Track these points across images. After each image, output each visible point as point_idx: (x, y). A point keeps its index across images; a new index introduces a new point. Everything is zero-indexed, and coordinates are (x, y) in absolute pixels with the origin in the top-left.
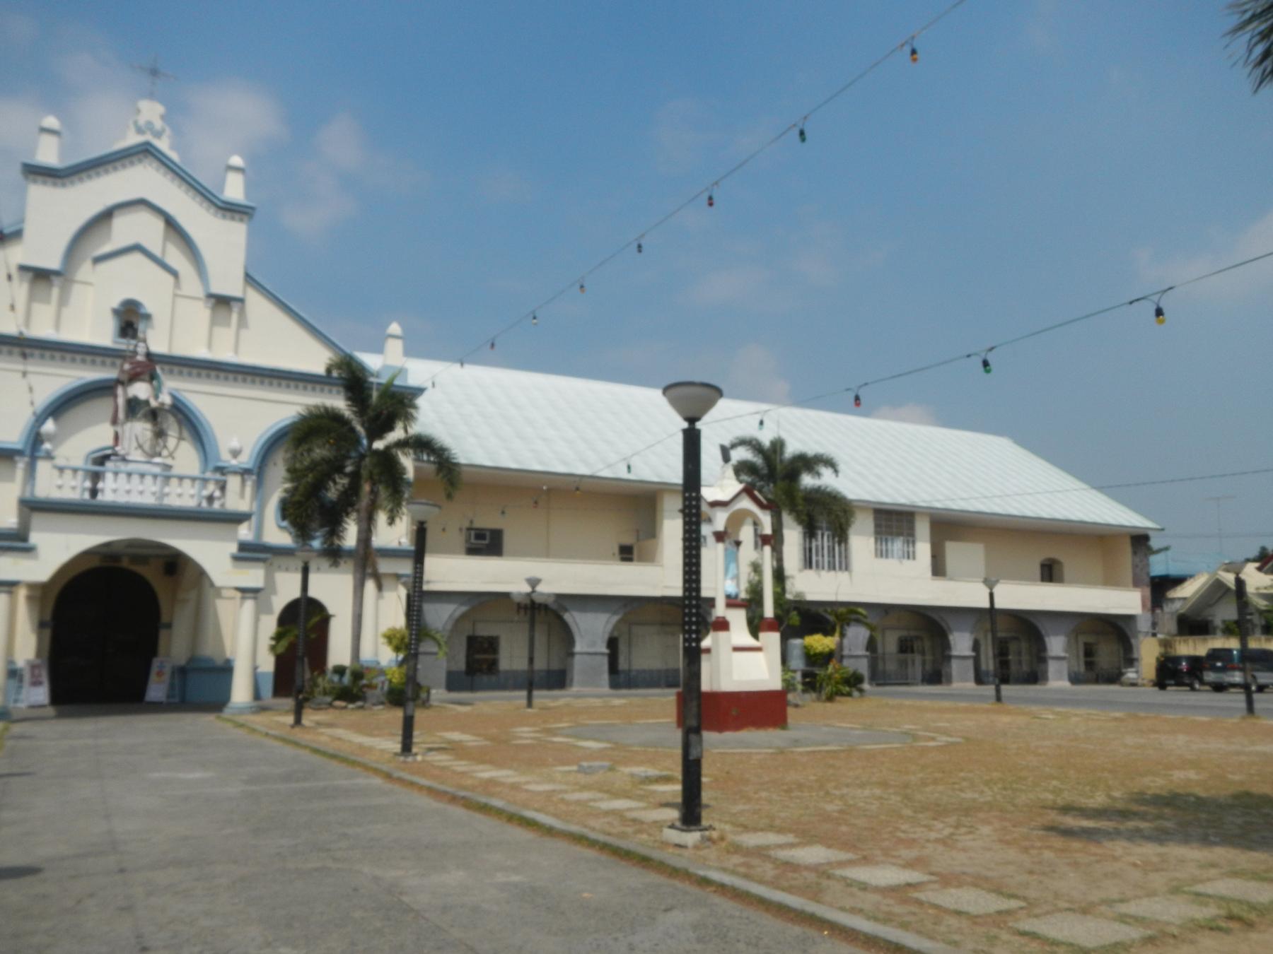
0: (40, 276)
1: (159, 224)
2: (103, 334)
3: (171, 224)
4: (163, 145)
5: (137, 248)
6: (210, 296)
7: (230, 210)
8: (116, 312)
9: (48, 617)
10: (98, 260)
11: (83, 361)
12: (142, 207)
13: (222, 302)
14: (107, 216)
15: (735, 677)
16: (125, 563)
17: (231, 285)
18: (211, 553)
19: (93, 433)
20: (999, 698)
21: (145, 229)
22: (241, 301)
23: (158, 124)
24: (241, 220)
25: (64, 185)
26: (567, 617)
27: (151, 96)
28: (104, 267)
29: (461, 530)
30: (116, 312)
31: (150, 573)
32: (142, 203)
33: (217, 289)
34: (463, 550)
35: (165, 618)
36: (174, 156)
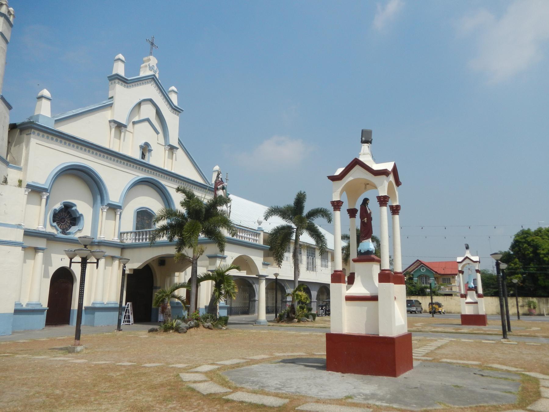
0: (120, 126)
1: (154, 111)
3: (159, 113)
4: (157, 76)
5: (148, 120)
6: (170, 145)
7: (176, 110)
8: (141, 147)
10: (134, 123)
11: (136, 168)
12: (149, 102)
13: (172, 148)
14: (139, 104)
15: (365, 308)
17: (174, 142)
20: (433, 316)
22: (177, 148)
23: (155, 68)
24: (178, 115)
25: (128, 87)
26: (254, 286)
27: (151, 54)
28: (137, 126)
30: (141, 147)
32: (151, 101)
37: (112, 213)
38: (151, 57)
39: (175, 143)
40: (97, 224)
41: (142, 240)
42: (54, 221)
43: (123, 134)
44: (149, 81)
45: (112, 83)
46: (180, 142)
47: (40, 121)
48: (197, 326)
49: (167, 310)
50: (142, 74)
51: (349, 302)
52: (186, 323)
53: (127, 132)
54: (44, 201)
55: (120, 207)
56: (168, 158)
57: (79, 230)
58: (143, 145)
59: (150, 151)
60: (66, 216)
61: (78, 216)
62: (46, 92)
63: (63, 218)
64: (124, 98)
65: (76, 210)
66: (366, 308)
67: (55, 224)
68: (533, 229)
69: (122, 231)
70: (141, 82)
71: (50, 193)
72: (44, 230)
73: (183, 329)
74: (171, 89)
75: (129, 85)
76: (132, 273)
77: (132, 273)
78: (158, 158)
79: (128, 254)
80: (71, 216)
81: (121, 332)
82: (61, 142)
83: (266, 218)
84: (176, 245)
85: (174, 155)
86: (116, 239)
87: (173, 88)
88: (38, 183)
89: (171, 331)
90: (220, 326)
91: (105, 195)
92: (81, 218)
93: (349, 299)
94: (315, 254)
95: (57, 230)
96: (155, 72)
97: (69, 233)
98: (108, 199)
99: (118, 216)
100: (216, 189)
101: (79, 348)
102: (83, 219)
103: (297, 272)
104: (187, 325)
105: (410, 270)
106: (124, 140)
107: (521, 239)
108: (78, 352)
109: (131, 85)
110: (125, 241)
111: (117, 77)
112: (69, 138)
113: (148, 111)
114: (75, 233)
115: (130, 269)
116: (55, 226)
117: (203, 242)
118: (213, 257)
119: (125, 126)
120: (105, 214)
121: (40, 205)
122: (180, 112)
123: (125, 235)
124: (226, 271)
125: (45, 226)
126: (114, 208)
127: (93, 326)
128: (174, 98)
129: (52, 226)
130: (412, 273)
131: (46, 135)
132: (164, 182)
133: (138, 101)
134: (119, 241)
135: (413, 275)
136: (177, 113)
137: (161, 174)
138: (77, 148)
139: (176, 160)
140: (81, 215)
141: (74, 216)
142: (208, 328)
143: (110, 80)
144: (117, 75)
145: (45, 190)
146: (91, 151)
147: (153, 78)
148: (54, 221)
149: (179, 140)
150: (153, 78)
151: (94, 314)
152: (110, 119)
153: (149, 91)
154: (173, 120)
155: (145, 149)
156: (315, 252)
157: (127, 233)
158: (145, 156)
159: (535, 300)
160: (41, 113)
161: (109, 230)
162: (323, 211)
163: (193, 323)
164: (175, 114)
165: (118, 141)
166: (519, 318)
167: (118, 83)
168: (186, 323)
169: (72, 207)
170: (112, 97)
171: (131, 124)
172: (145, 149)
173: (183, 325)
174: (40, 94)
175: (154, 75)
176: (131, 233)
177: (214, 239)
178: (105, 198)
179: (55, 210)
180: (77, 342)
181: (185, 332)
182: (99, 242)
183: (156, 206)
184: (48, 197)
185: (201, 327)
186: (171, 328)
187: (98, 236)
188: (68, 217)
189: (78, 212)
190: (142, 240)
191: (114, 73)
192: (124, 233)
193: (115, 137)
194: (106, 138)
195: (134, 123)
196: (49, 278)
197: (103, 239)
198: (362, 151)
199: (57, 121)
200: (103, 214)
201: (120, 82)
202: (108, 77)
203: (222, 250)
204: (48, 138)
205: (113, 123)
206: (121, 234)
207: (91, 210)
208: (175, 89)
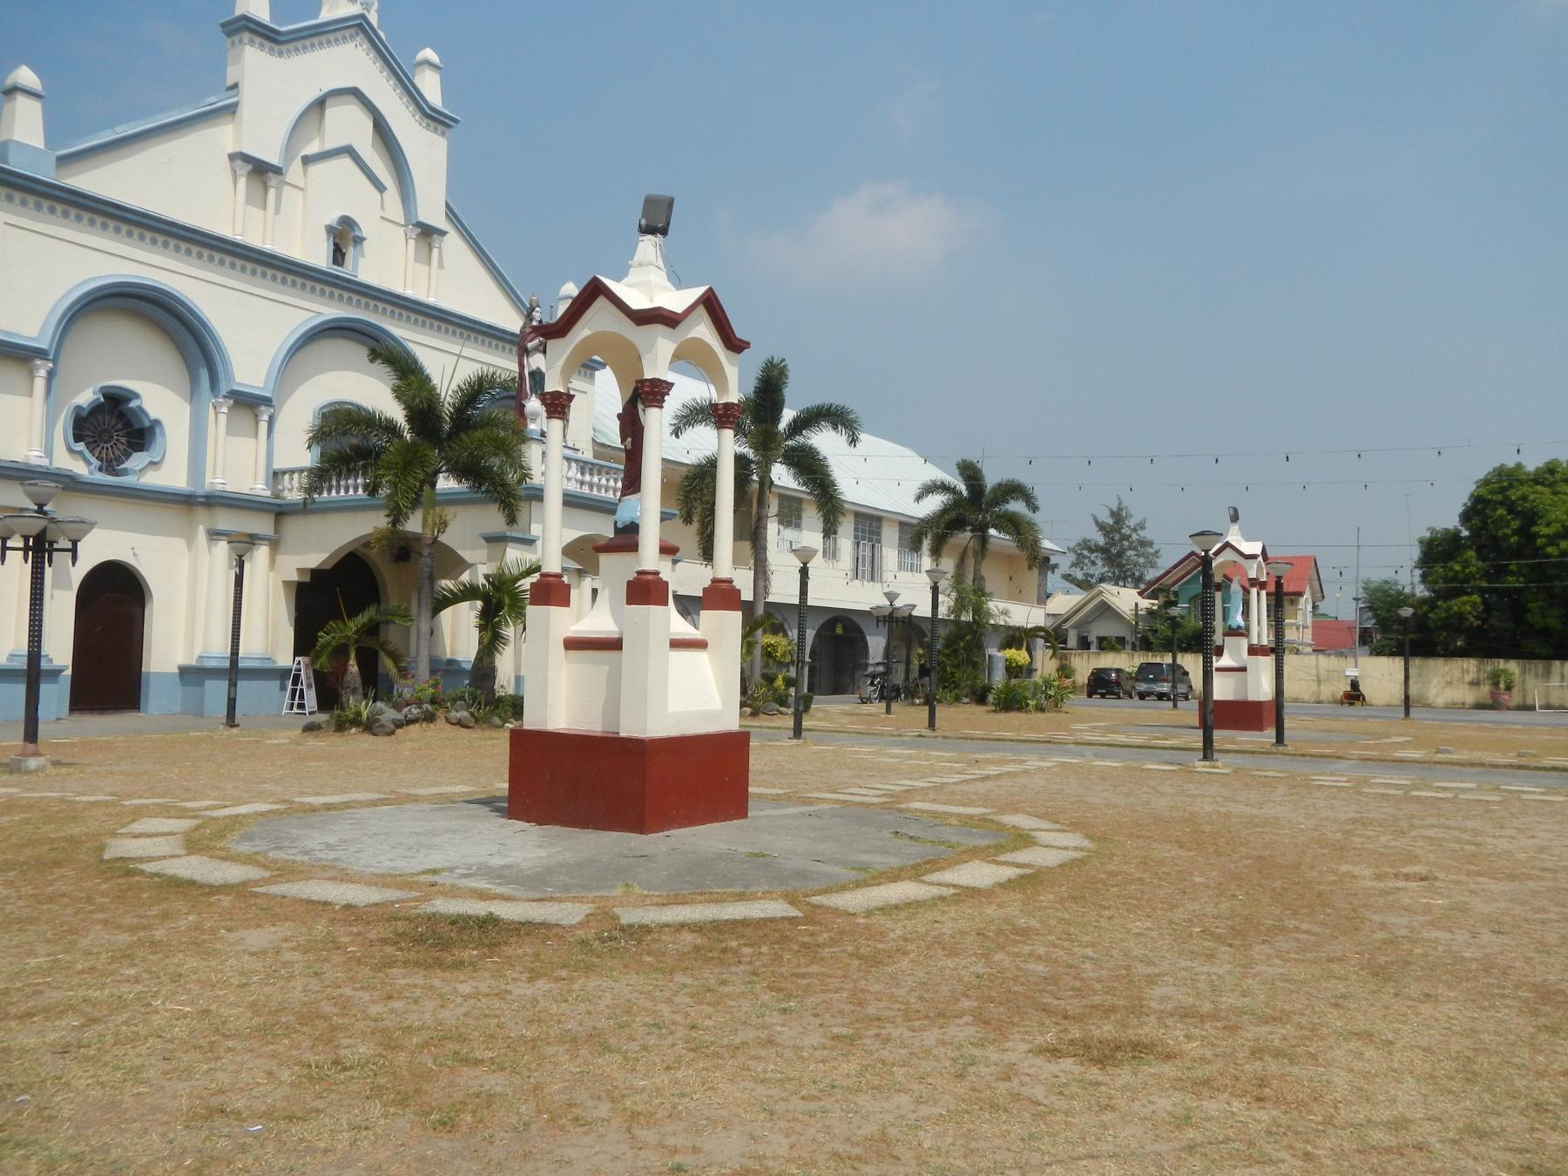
0: (261, 171)
2: (317, 255)
3: (381, 129)
4: (373, 18)
5: (349, 151)
6: (419, 225)
7: (435, 119)
8: (330, 230)
10: (307, 160)
12: (352, 98)
13: (427, 233)
14: (320, 104)
22: (443, 233)
24: (443, 134)
25: (280, 54)
28: (316, 169)
30: (330, 230)
32: (355, 93)
37: (244, 417)
39: (438, 219)
40: (192, 444)
41: (347, 491)
42: (77, 438)
43: (272, 193)
44: (347, 33)
45: (233, 44)
46: (451, 214)
47: (11, 159)
48: (430, 718)
49: (348, 677)
50: (326, 15)
51: (572, 653)
52: (399, 710)
53: (286, 187)
54: (40, 384)
55: (267, 401)
56: (416, 260)
57: (152, 463)
58: (334, 224)
59: (359, 241)
60: (114, 426)
61: (147, 424)
62: (26, 76)
63: (105, 431)
64: (272, 87)
65: (139, 407)
66: (607, 668)
67: (81, 446)
68: (1532, 464)
69: (277, 466)
70: (323, 39)
71: (55, 361)
72: (45, 462)
73: (383, 726)
74: (421, 56)
75: (283, 48)
76: (307, 579)
77: (307, 579)
78: (386, 263)
79: (294, 528)
80: (128, 424)
81: (235, 730)
82: (92, 223)
83: (677, 432)
84: (386, 507)
85: (435, 252)
86: (258, 487)
87: (429, 54)
88: (22, 337)
89: (353, 730)
90: (496, 720)
91: (220, 368)
92: (158, 430)
93: (573, 644)
94: (879, 534)
95: (89, 463)
96: (367, 7)
97: (125, 472)
98: (230, 378)
99: (263, 426)
100: (524, 352)
101: (33, 763)
102: (163, 433)
103: (761, 583)
104: (400, 716)
105: (1167, 581)
106: (277, 211)
107: (1493, 492)
108: (28, 772)
109: (291, 46)
110: (286, 494)
111: (245, 26)
112: (101, 207)
113: (348, 126)
114: (141, 471)
115: (300, 571)
116: (80, 453)
117: (453, 500)
118: (496, 540)
119: (278, 171)
120: (223, 419)
121: (31, 395)
122: (449, 126)
123: (296, 476)
124: (518, 579)
125: (49, 452)
126: (248, 404)
127: (202, 715)
128: (430, 86)
129: (71, 451)
130: (1175, 588)
131: (31, 200)
132: (403, 332)
133: (315, 94)
134: (268, 493)
135: (1176, 594)
136: (440, 128)
137: (389, 308)
138: (130, 234)
139: (441, 265)
140: (157, 422)
141: (137, 426)
142: (460, 723)
143: (229, 34)
144: (245, 18)
145: (41, 354)
146: (172, 242)
147: (360, 25)
148: (77, 438)
149: (447, 206)
150: (359, 26)
151: (202, 684)
152: (231, 150)
153: (350, 63)
154: (426, 152)
155: (343, 236)
156: (879, 527)
157: (292, 472)
158: (343, 255)
159: (1513, 666)
160: (16, 138)
161: (239, 464)
162: (835, 414)
163: (415, 711)
164: (435, 131)
165: (256, 212)
166: (1407, 713)
167: (252, 42)
168: (399, 710)
169: (129, 400)
170: (235, 86)
171: (298, 163)
172: (343, 236)
173: (389, 714)
174: (9, 81)
175: (363, 16)
176: (301, 471)
177: (487, 491)
178: (221, 376)
179: (78, 408)
180: (31, 746)
181: (392, 733)
182: (207, 497)
183: (376, 394)
184: (51, 375)
185: (441, 722)
186: (356, 721)
187: (208, 479)
188: (119, 426)
189: (146, 414)
190: (347, 491)
191: (238, 12)
192: (284, 473)
193: (249, 201)
194: (224, 210)
195: (307, 160)
196: (70, 588)
197: (220, 487)
198: (637, 258)
199: (62, 161)
200: (218, 419)
201: (258, 40)
202: (223, 25)
203: (512, 520)
204: (38, 207)
205: (239, 162)
206: (276, 475)
207: (187, 408)
208: (435, 58)
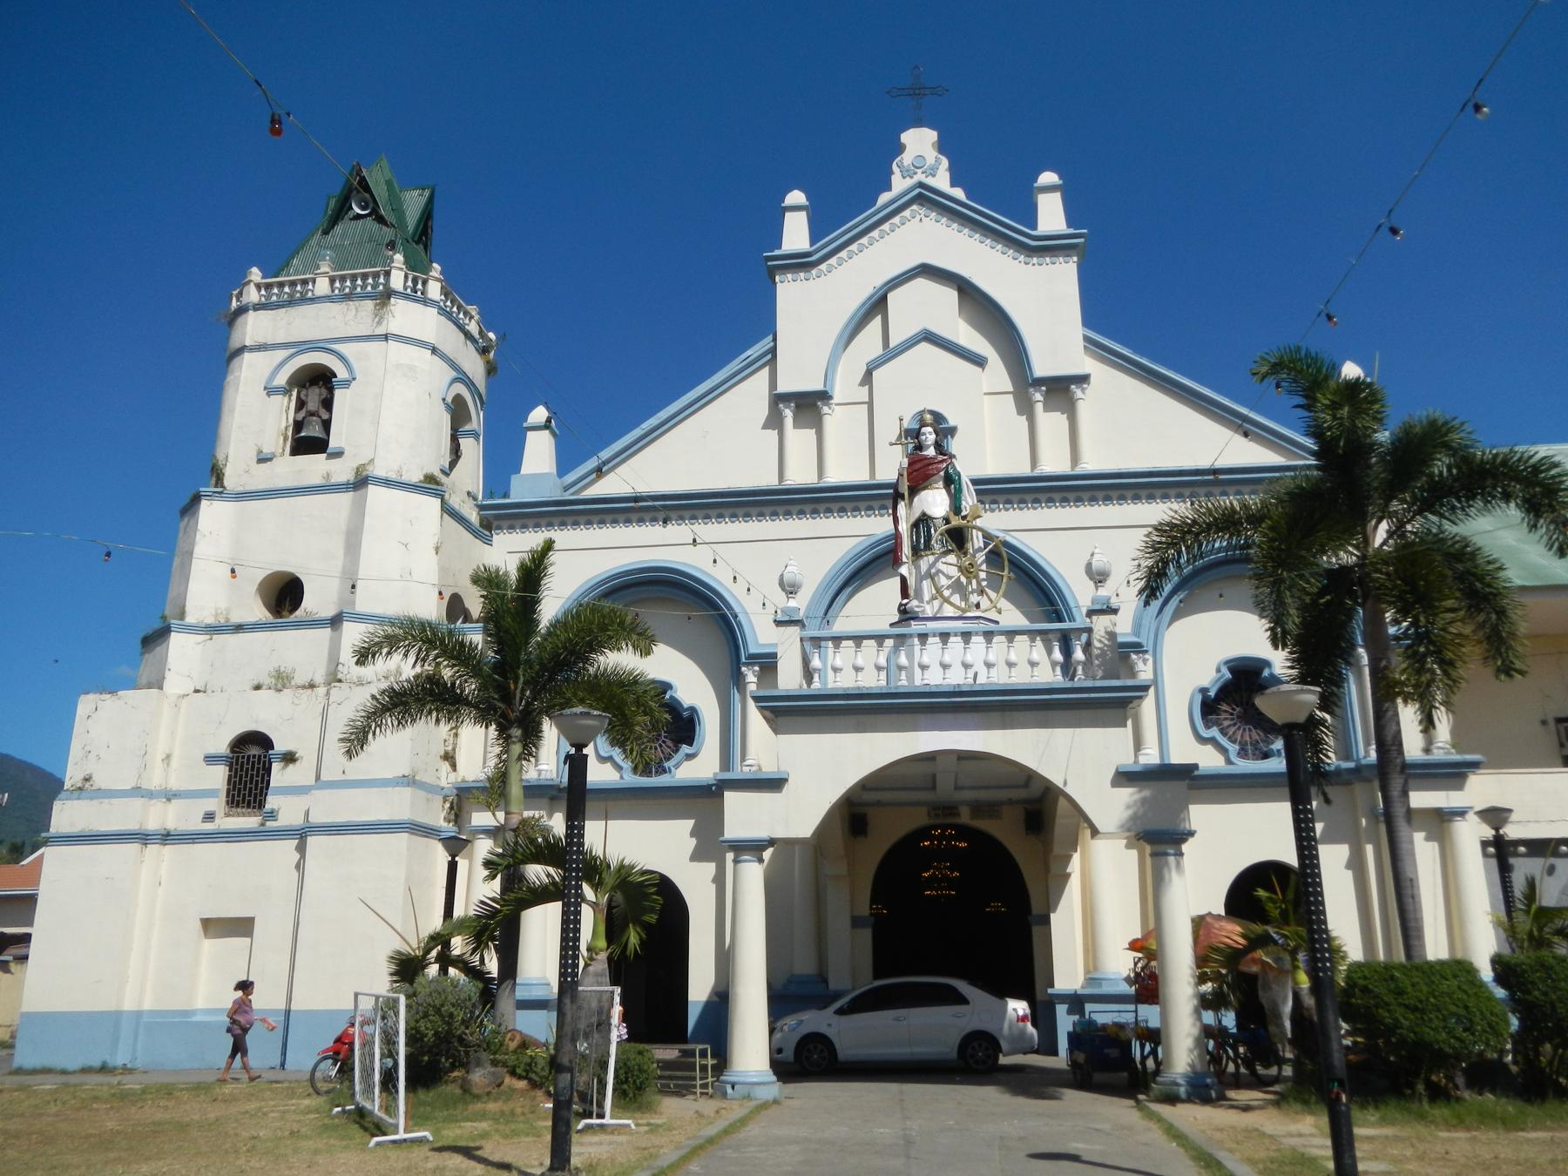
1: (951, 295)
3: (968, 292)
4: (942, 181)
5: (929, 337)
9: (864, 909)
14: (878, 305)
16: (965, 818)
18: (1080, 764)
19: (877, 603)
21: (930, 306)
22: (1083, 379)
23: (931, 155)
27: (918, 123)
29: (1544, 723)
31: (1006, 831)
33: (1042, 366)
34: (1560, 760)
35: (1036, 908)
36: (959, 193)
38: (907, 137)
44: (907, 213)
95: (619, 768)
119: (824, 396)
140: (693, 710)
147: (920, 195)
149: (1087, 339)
175: (921, 185)
